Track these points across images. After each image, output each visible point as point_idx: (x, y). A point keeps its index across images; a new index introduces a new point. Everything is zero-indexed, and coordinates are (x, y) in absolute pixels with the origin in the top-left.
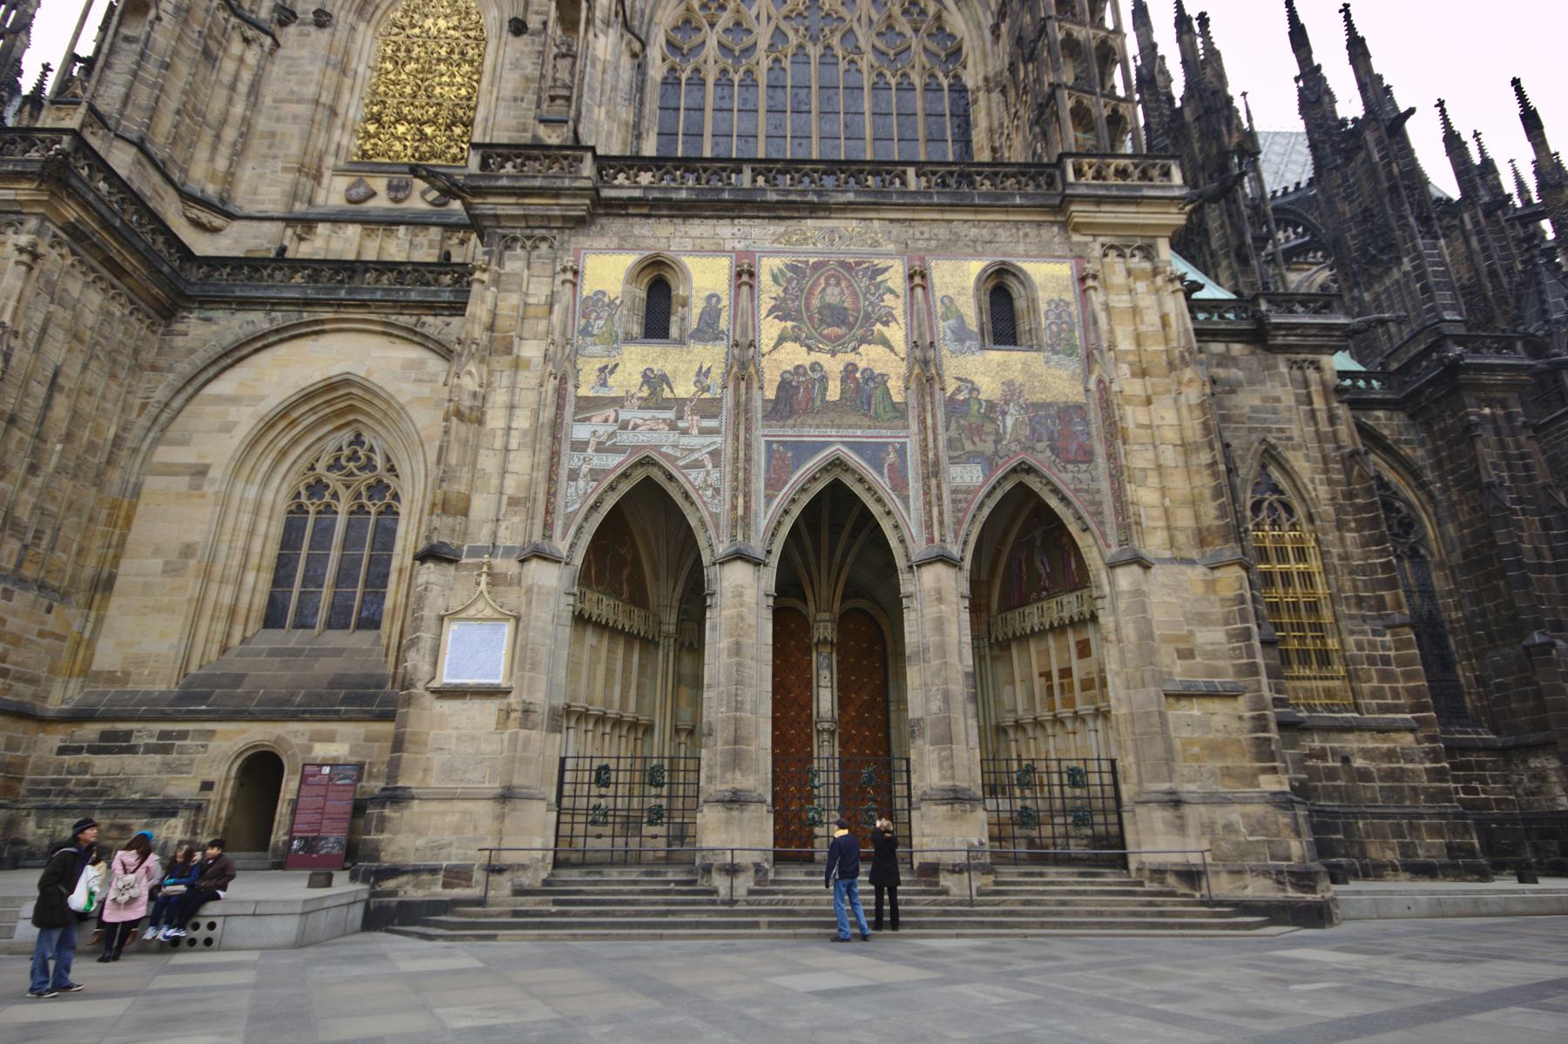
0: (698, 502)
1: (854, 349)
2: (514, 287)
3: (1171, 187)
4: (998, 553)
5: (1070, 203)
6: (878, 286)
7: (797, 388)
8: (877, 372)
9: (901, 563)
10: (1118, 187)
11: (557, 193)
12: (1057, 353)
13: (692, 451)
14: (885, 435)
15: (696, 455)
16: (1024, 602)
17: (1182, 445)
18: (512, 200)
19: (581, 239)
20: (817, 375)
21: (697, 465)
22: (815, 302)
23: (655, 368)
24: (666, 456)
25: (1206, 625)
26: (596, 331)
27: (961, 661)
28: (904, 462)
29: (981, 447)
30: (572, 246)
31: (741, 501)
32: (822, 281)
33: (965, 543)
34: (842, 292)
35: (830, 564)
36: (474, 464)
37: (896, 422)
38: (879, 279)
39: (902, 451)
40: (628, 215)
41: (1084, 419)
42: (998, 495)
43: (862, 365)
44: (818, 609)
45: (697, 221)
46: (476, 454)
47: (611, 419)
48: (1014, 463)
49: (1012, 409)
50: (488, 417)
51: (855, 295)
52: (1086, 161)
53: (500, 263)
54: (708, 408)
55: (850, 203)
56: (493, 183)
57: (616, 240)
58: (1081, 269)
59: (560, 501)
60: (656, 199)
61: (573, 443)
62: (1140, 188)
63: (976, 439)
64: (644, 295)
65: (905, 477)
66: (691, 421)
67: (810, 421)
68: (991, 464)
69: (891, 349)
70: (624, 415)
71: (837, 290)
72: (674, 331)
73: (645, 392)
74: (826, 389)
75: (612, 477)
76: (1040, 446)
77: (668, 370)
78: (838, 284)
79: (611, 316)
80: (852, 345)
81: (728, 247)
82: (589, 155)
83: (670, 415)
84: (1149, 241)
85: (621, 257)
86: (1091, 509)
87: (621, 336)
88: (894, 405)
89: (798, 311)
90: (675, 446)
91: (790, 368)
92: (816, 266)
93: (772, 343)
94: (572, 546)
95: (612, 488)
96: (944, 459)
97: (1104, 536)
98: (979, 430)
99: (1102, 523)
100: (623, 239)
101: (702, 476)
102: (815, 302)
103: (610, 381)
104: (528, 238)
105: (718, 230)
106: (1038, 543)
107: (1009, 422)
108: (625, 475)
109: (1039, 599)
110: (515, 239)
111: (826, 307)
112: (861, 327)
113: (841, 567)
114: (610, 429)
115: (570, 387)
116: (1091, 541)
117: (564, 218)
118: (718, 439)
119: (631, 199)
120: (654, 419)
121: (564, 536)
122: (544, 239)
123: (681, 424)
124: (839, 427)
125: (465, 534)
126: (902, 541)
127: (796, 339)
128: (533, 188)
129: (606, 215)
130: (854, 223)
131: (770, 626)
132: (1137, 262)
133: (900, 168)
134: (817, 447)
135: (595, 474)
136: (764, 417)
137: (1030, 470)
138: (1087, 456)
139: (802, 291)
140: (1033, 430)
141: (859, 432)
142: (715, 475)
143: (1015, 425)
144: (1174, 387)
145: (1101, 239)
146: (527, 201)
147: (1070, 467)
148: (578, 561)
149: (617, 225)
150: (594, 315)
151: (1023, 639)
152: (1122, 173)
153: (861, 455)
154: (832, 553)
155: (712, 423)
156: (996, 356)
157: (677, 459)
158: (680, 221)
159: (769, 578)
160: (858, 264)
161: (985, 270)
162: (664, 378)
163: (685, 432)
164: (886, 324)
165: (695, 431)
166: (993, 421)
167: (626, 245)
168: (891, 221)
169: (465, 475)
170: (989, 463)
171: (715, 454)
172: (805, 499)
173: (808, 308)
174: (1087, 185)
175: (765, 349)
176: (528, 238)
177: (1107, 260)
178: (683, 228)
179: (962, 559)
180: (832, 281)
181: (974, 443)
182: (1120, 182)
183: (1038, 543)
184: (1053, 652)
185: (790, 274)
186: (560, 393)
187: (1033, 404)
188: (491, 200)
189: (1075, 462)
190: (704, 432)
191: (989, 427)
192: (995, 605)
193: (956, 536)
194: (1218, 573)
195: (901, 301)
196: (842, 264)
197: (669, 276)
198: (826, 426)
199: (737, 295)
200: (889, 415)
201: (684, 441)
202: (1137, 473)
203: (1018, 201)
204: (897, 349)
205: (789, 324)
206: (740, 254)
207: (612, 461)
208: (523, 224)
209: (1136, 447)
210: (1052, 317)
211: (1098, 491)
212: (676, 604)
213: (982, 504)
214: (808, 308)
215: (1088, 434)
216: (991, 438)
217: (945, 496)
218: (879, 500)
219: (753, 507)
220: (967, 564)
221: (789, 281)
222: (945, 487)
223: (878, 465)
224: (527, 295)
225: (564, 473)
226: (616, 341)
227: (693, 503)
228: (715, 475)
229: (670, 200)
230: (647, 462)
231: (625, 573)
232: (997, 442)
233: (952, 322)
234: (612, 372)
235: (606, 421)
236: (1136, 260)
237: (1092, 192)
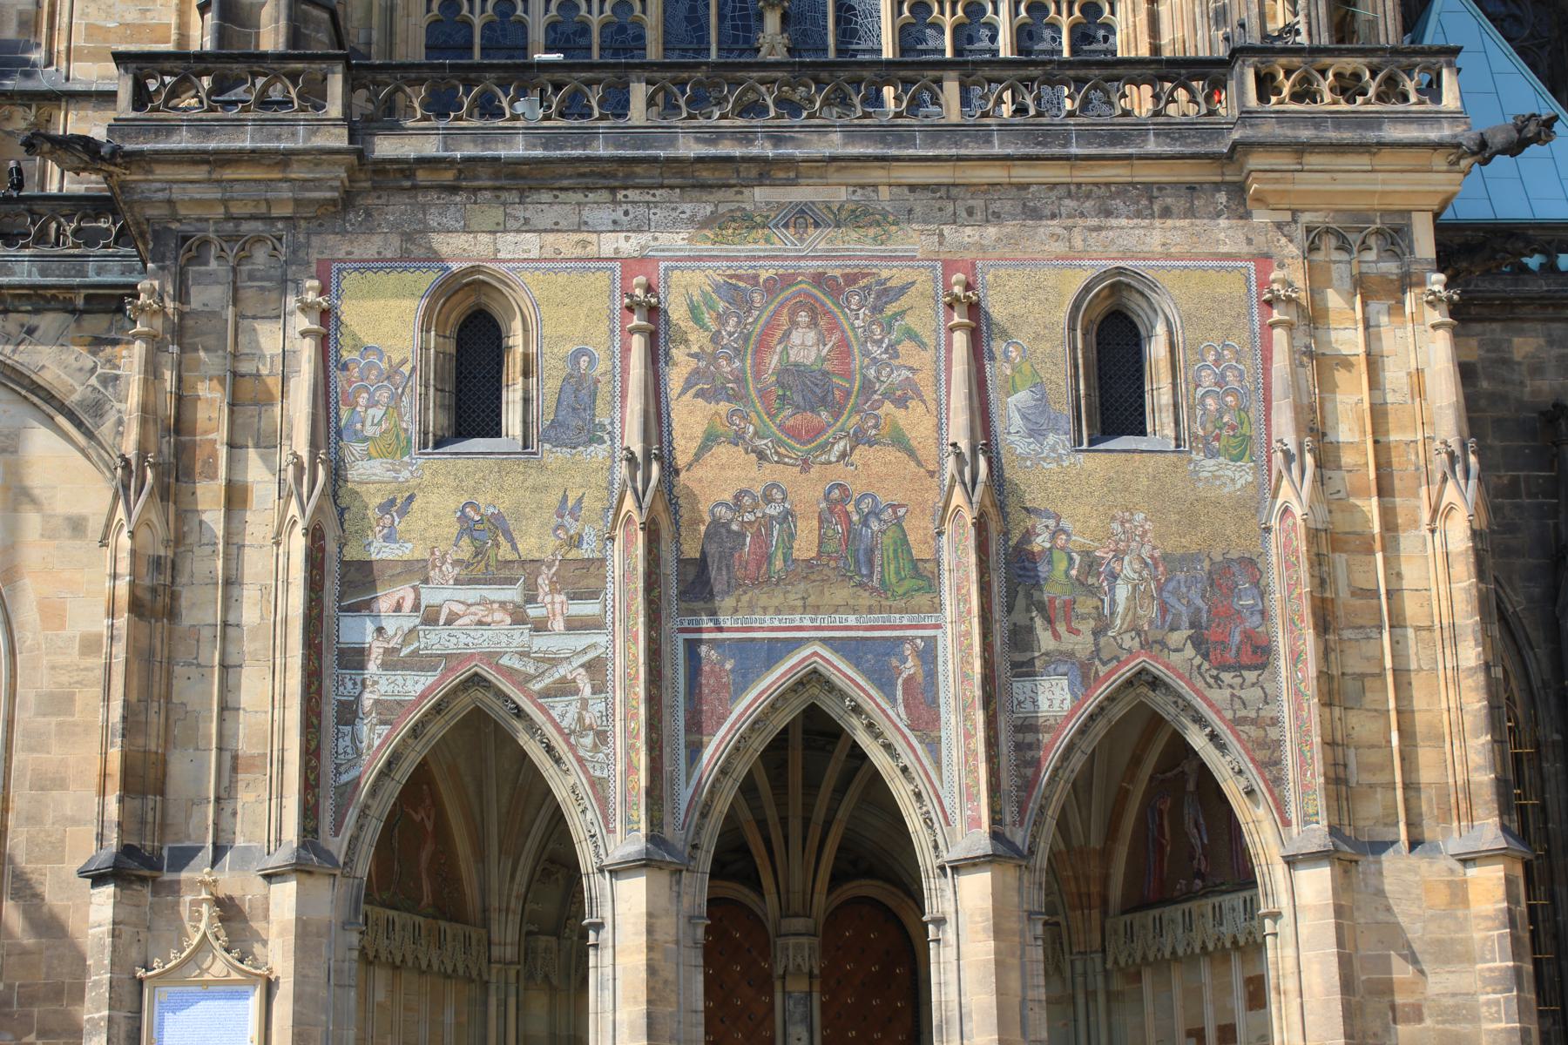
0: (568, 758)
1: (843, 455)
2: (211, 341)
3: (1435, 119)
4: (1123, 796)
5: (1246, 154)
6: (888, 328)
7: (741, 535)
8: (883, 500)
9: (926, 860)
10: (1338, 120)
11: (285, 158)
12: (1213, 454)
13: (554, 662)
14: (896, 623)
15: (562, 671)
16: (1165, 899)
17: (1430, 629)
18: (200, 173)
19: (331, 239)
20: (773, 510)
21: (565, 688)
22: (774, 361)
23: (481, 500)
24: (509, 673)
25: (1448, 962)
26: (369, 431)
27: (1024, 1034)
28: (932, 675)
29: (1069, 642)
30: (314, 256)
31: (642, 760)
32: (784, 319)
33: (1038, 823)
34: (822, 341)
35: (806, 823)
36: (168, 698)
37: (922, 599)
38: (891, 309)
39: (928, 654)
40: (414, 187)
41: (1256, 584)
42: (1100, 728)
43: (856, 488)
44: (785, 912)
45: (546, 196)
46: (170, 675)
47: (408, 605)
48: (1126, 671)
49: (1128, 568)
50: (184, 602)
51: (844, 347)
52: (1279, 65)
53: (182, 295)
54: (582, 579)
55: (833, 159)
56: (161, 146)
57: (395, 241)
58: (1263, 283)
59: (327, 766)
60: (468, 160)
61: (342, 653)
62: (1375, 121)
63: (1061, 628)
64: (451, 347)
65: (934, 703)
66: (554, 605)
67: (764, 600)
68: (1085, 677)
69: (911, 453)
70: (429, 597)
71: (811, 336)
72: (512, 419)
73: (466, 550)
74: (792, 536)
75: (415, 716)
76: (1176, 638)
77: (504, 504)
78: (813, 323)
79: (396, 398)
80: (839, 447)
81: (607, 251)
82: (339, 68)
83: (513, 594)
84: (1398, 221)
85: (407, 276)
86: (1261, 755)
87: (415, 439)
88: (915, 563)
89: (740, 379)
90: (524, 655)
91: (728, 497)
92: (773, 287)
93: (693, 446)
94: (354, 841)
95: (416, 732)
96: (1003, 667)
97: (1280, 806)
98: (1069, 606)
99: (1276, 783)
100: (408, 237)
101: (573, 711)
102: (774, 361)
103: (400, 526)
104: (231, 238)
105: (586, 212)
106: (1191, 787)
107: (1122, 592)
108: (438, 709)
109: (1190, 896)
110: (205, 243)
111: (792, 373)
112: (856, 410)
113: (828, 825)
114: (407, 624)
115: (331, 546)
116: (1261, 812)
117: (298, 202)
118: (601, 639)
119: (422, 161)
120: (483, 602)
121: (337, 828)
122: (260, 240)
123: (533, 612)
124: (817, 609)
125: (163, 825)
126: (928, 822)
127: (737, 439)
128: (241, 151)
129: (374, 188)
130: (842, 194)
131: (701, 978)
132: (1376, 263)
133: (931, 74)
134: (775, 650)
135: (388, 710)
136: (682, 595)
137: (1155, 683)
138: (1260, 654)
139: (747, 339)
140: (1164, 609)
141: (852, 620)
142: (597, 706)
143: (1132, 597)
144: (1425, 516)
145: (1306, 218)
146: (229, 174)
147: (1227, 677)
148: (363, 867)
149: (396, 208)
150: (363, 399)
151: (1163, 965)
152: (1348, 87)
153: (857, 664)
154: (811, 786)
155: (589, 608)
156: (1098, 464)
157: (529, 678)
158: (513, 197)
159: (697, 889)
160: (851, 279)
161: (1087, 289)
162: (498, 525)
163: (540, 627)
164: (902, 402)
165: (559, 625)
166: (1092, 591)
167: (418, 252)
168: (913, 188)
169: (155, 720)
170: (1084, 675)
171: (595, 667)
172: (759, 744)
173: (757, 376)
174: (1282, 117)
175: (682, 460)
176: (231, 238)
177: (1319, 257)
178: (519, 211)
179: (1031, 852)
180: (803, 317)
181: (1056, 635)
182: (1344, 107)
183: (1191, 787)
184: (1208, 995)
185: (721, 305)
186: (315, 560)
187: (1165, 557)
188: (163, 173)
189: (1238, 667)
190: (575, 625)
191: (1086, 605)
192: (1116, 892)
193: (1022, 810)
194: (1472, 872)
195: (928, 355)
196: (819, 279)
197: (496, 309)
198: (793, 610)
199: (626, 350)
200: (908, 584)
201: (541, 643)
202: (1349, 682)
203: (1152, 146)
204: (922, 454)
205: (724, 407)
206: (631, 264)
207: (415, 686)
208: (220, 211)
209: (1347, 634)
210: (1208, 380)
211: (1275, 722)
212: (515, 904)
213: (1070, 748)
214: (757, 376)
215: (1263, 613)
216: (1086, 627)
217: (1002, 738)
218: (888, 747)
219: (667, 768)
220: (1041, 859)
221: (721, 319)
222: (1003, 721)
223: (885, 683)
224: (235, 356)
225: (329, 711)
226: (406, 450)
227: (558, 761)
228: (597, 706)
229: (497, 159)
230: (476, 680)
231: (425, 856)
232: (1096, 633)
233: (1023, 397)
234: (403, 512)
235: (398, 608)
236: (1371, 256)
237: (1287, 133)
